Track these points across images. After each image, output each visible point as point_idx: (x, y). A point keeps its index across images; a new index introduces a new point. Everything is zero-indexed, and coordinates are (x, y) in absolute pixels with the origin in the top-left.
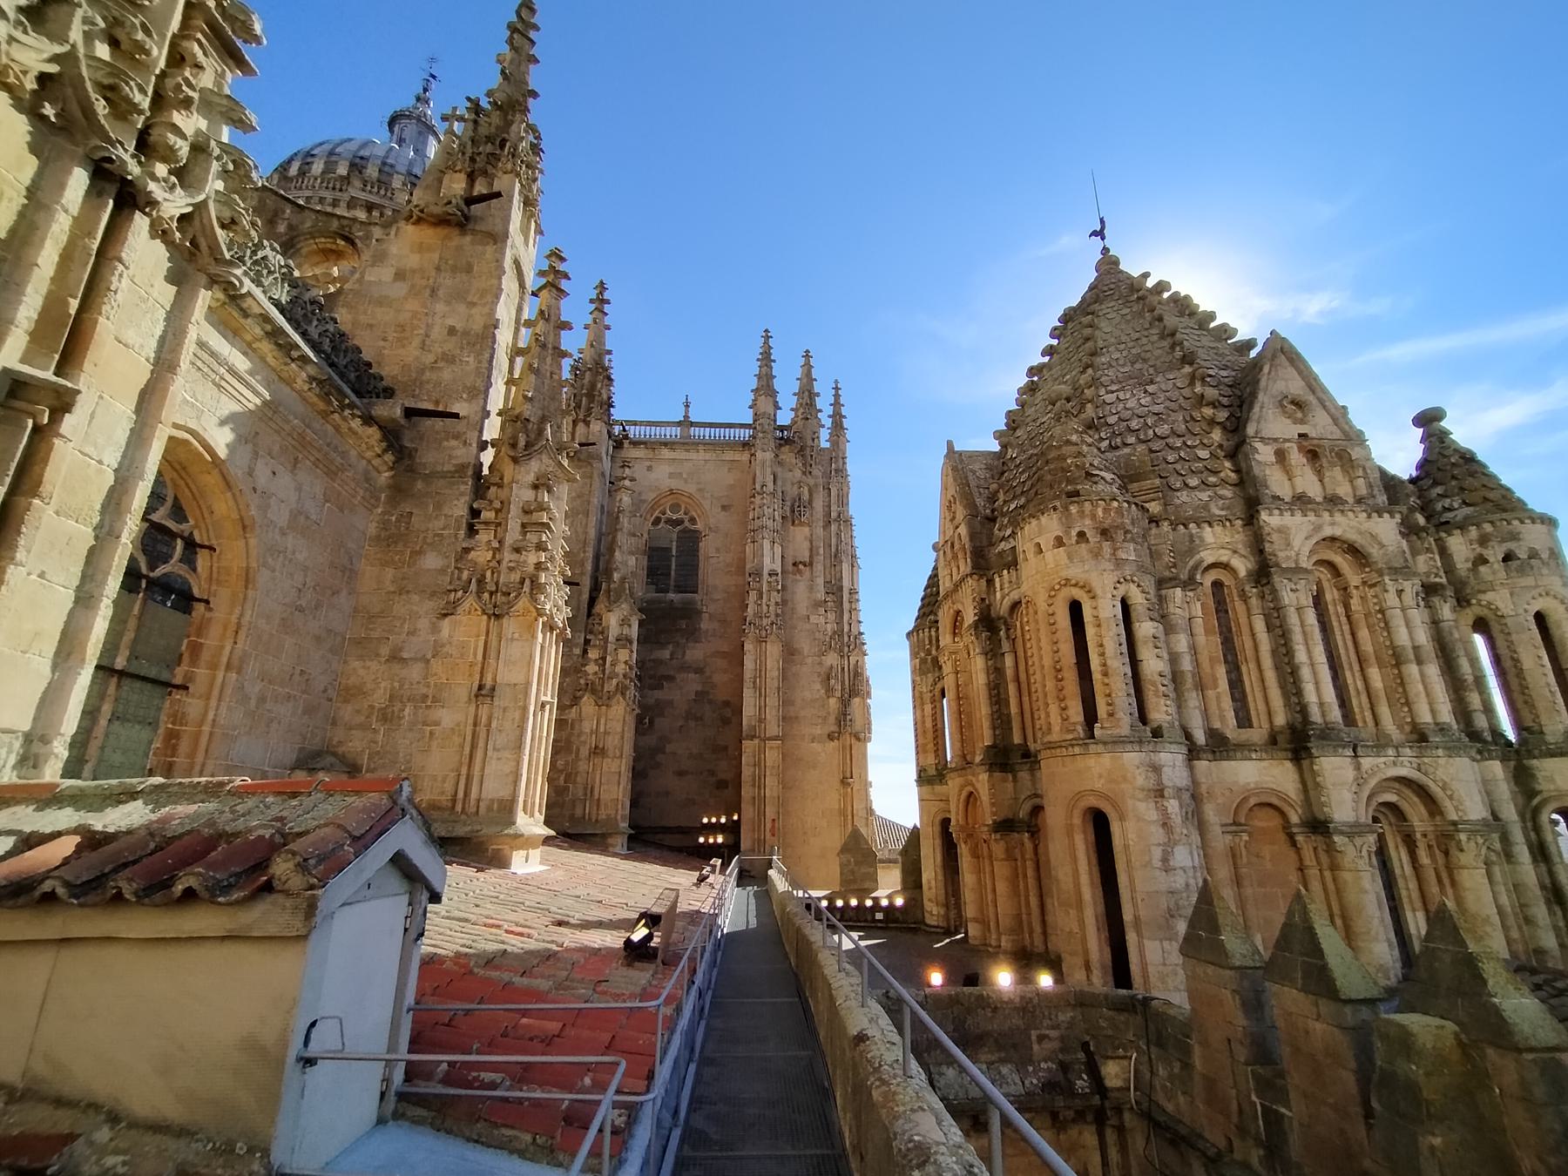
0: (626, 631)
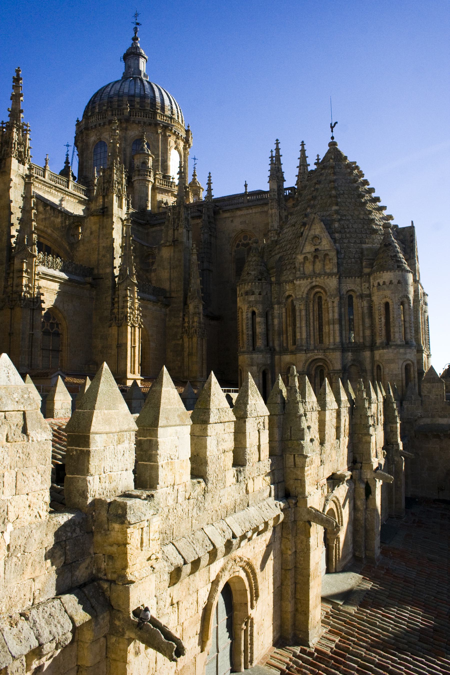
0: (197, 310)
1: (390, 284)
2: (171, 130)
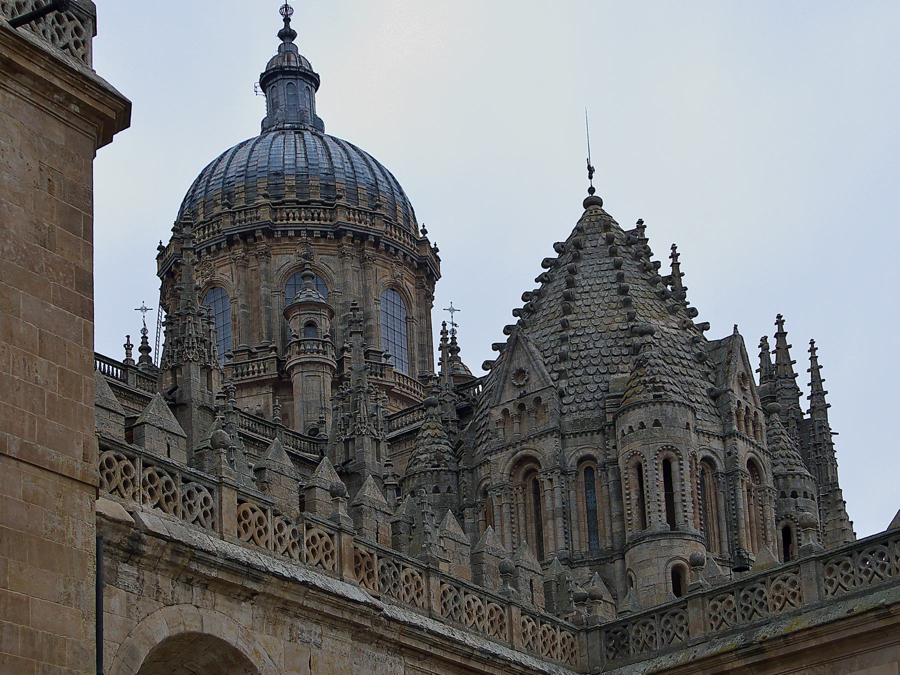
1: (639, 428)
2: (376, 244)
